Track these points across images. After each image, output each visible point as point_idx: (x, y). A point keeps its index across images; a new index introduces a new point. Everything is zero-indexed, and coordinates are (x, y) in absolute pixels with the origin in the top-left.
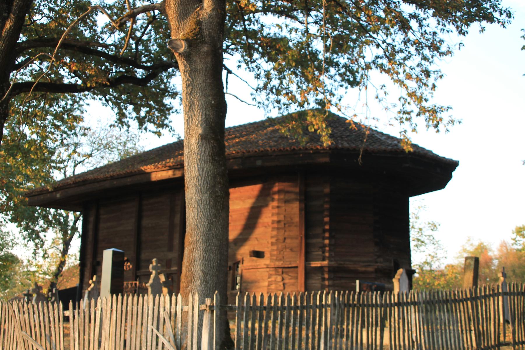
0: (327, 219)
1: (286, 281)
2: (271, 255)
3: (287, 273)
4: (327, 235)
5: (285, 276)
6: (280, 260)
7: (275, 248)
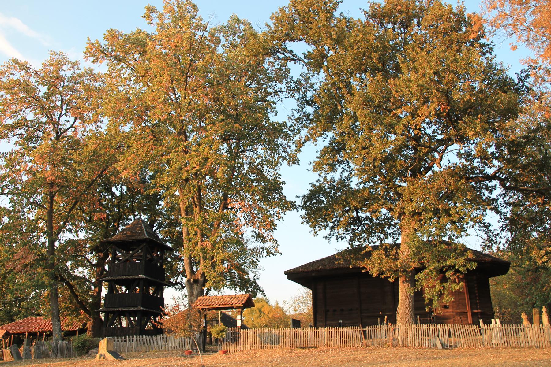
0: (476, 291)
1: (462, 319)
2: (453, 307)
3: (462, 315)
4: (477, 298)
5: (461, 316)
6: (458, 309)
7: (455, 304)
